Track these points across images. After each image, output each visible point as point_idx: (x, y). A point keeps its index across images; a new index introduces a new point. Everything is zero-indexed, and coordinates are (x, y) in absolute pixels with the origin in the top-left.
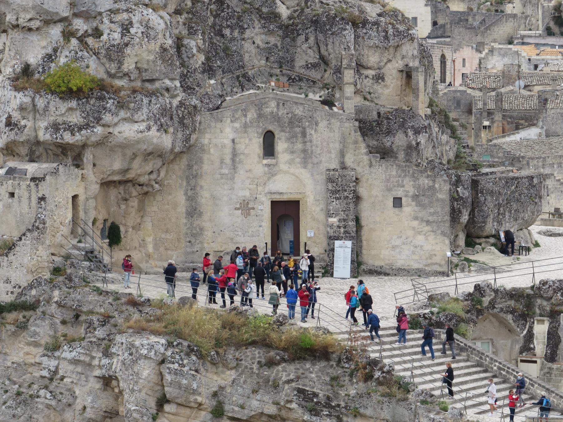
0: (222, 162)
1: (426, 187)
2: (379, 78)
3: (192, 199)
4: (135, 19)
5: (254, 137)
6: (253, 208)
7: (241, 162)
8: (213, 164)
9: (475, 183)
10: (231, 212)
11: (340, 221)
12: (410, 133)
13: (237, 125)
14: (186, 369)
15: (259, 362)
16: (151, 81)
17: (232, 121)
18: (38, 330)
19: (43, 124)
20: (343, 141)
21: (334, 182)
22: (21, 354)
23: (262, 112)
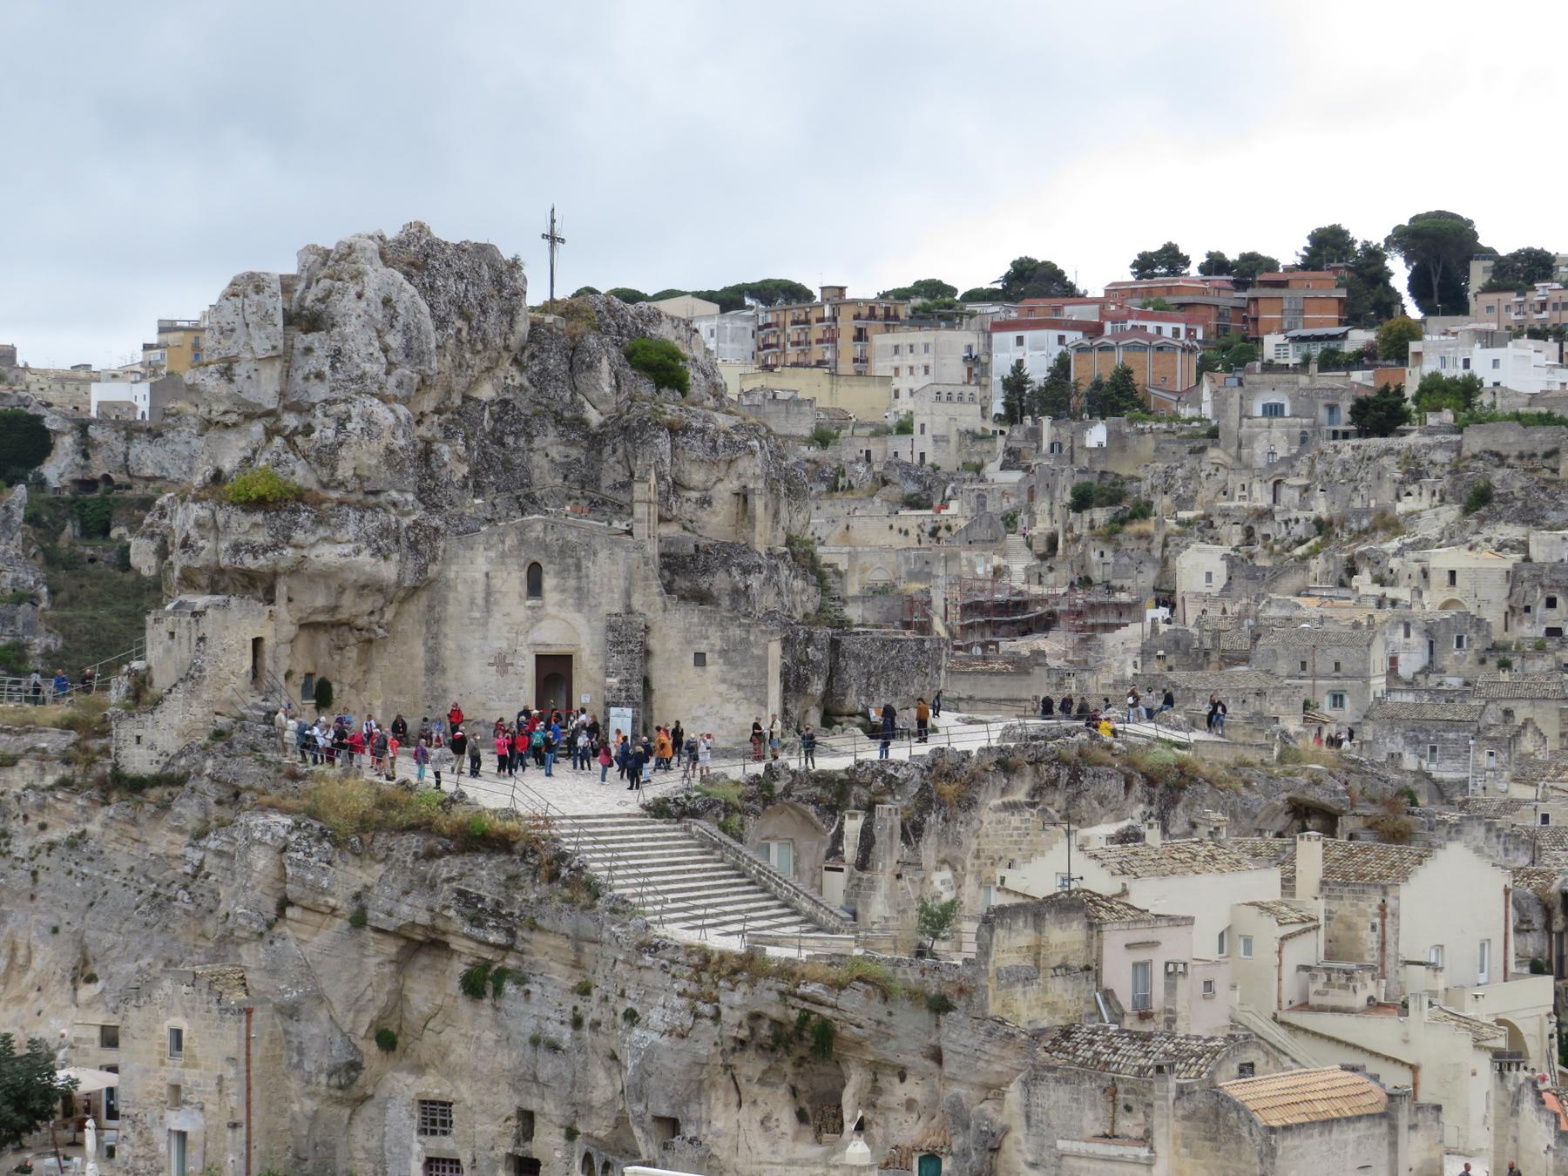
0: (472, 602)
2: (705, 502)
3: (433, 650)
4: (354, 412)
7: (496, 603)
9: (835, 644)
11: (621, 682)
12: (735, 572)
13: (492, 554)
14: (312, 860)
15: (415, 853)
16: (376, 493)
18: (183, 811)
19: (224, 545)
20: (630, 579)
22: (164, 844)
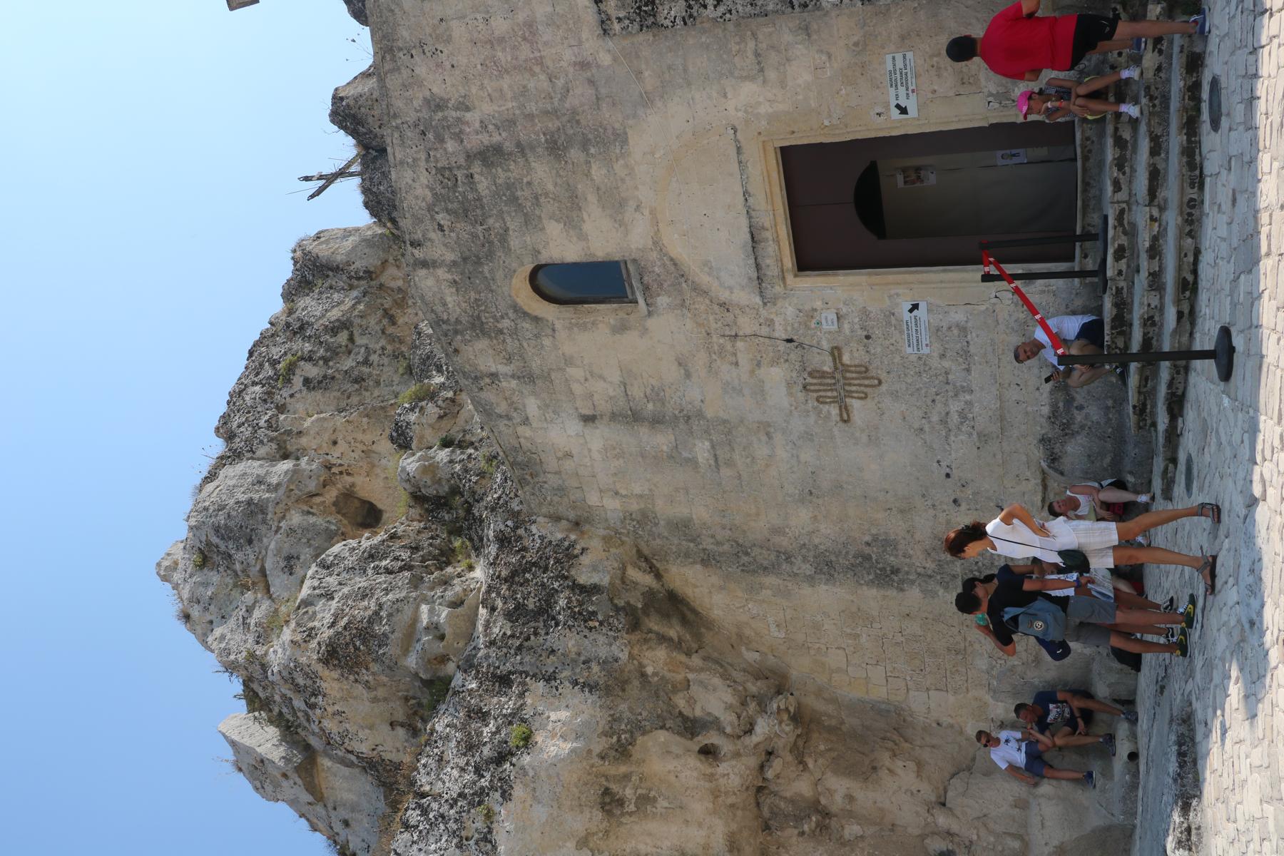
6: (836, 352)
7: (656, 395)
8: (687, 491)
10: (864, 439)
13: (532, 406)
23: (464, 319)
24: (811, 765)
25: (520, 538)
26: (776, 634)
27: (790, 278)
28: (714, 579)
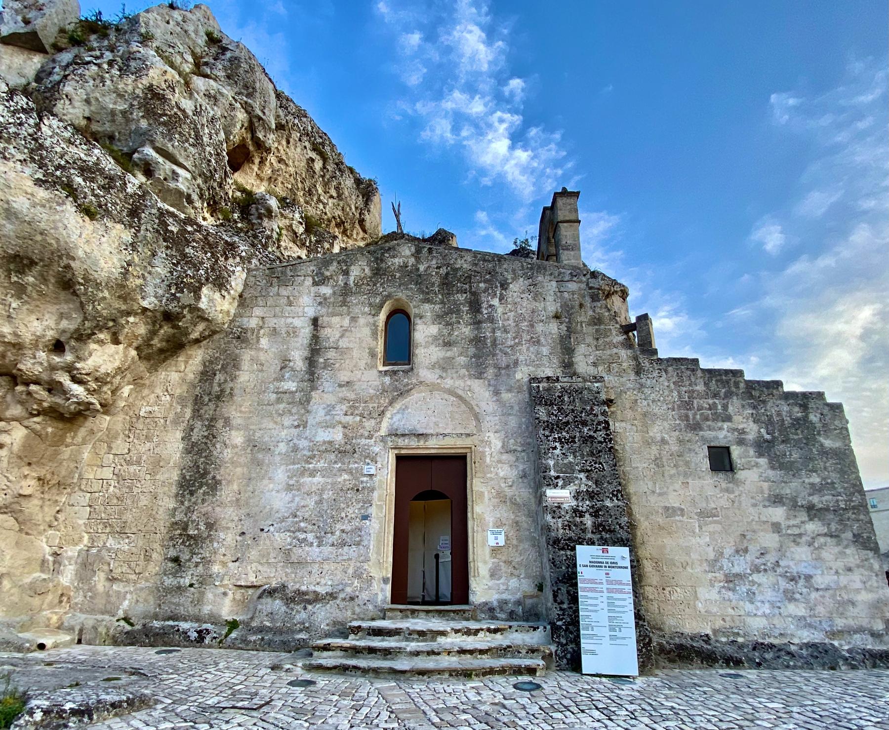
0: (285, 363)
1: (788, 421)
5: (363, 314)
8: (262, 371)
10: (291, 482)
11: (577, 496)
13: (326, 290)
17: (315, 284)
21: (551, 404)
24: (36, 419)
25: (234, 258)
26: (143, 410)
27: (396, 452)
28: (191, 376)
